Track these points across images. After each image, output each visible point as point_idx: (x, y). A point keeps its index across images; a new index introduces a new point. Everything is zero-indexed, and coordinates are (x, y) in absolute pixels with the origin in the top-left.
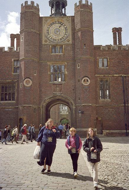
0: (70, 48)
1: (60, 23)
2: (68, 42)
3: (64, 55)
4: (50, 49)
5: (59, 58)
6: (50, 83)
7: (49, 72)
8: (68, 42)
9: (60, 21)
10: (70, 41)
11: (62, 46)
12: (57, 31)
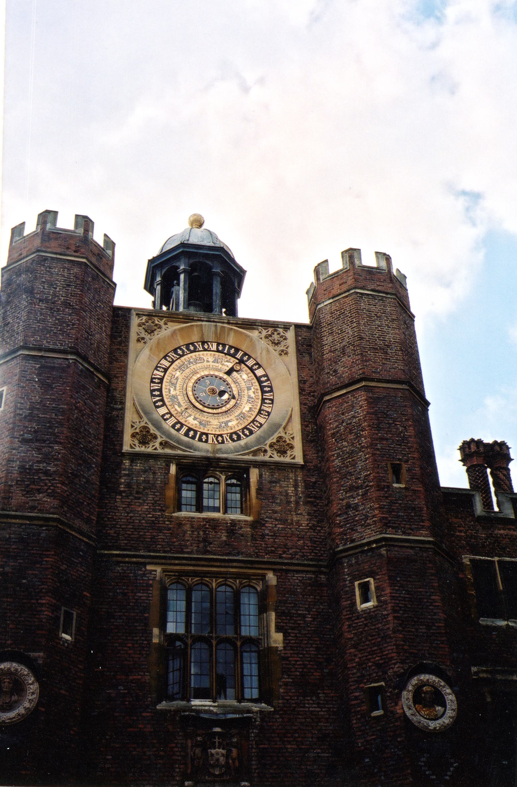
0: (291, 490)
1: (233, 351)
2: (282, 452)
3: (256, 525)
4: (166, 483)
5: (226, 543)
6: (164, 713)
7: (156, 631)
8: (282, 452)
9: (231, 340)
10: (292, 447)
11: (247, 471)
12: (213, 391)
